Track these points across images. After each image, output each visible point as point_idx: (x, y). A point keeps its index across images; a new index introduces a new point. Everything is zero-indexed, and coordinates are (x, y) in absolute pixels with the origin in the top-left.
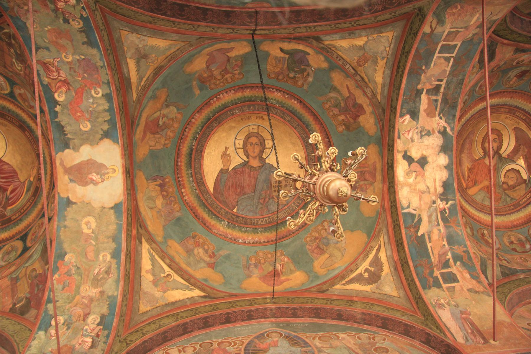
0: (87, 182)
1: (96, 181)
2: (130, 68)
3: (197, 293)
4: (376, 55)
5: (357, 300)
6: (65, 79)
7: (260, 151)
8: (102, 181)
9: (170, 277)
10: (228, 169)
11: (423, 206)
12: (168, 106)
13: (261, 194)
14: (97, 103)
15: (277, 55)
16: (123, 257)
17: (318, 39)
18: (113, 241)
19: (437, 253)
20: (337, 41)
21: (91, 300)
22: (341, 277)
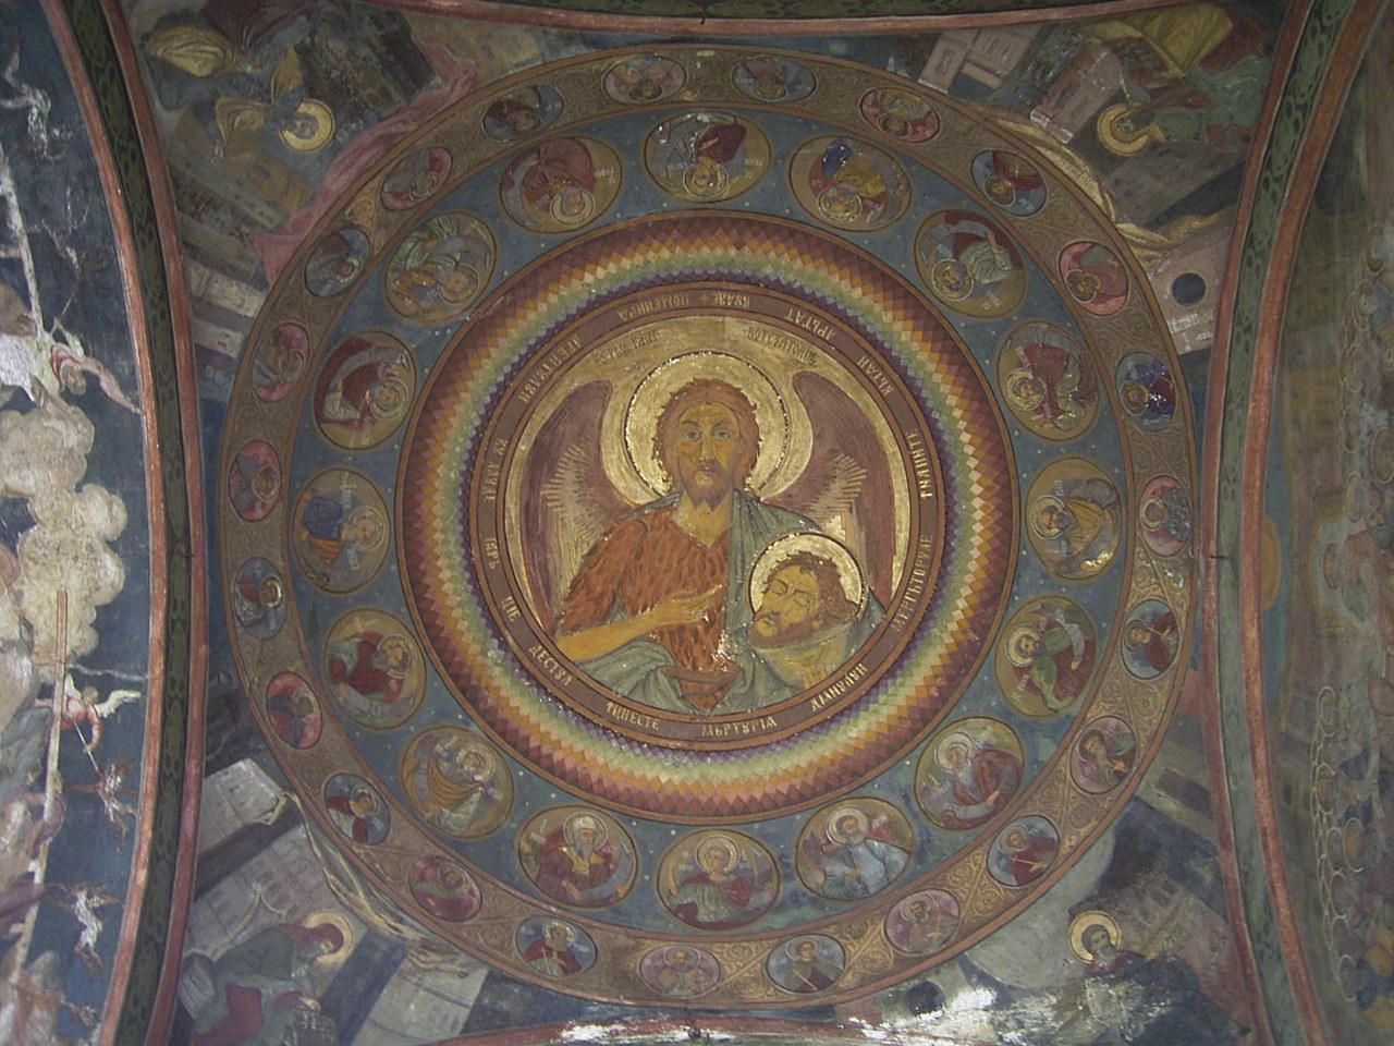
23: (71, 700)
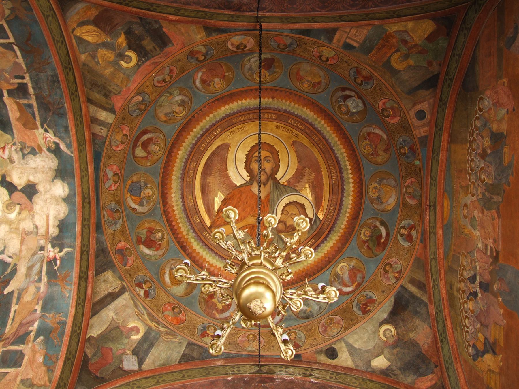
19: (19, 321)
23: (51, 252)
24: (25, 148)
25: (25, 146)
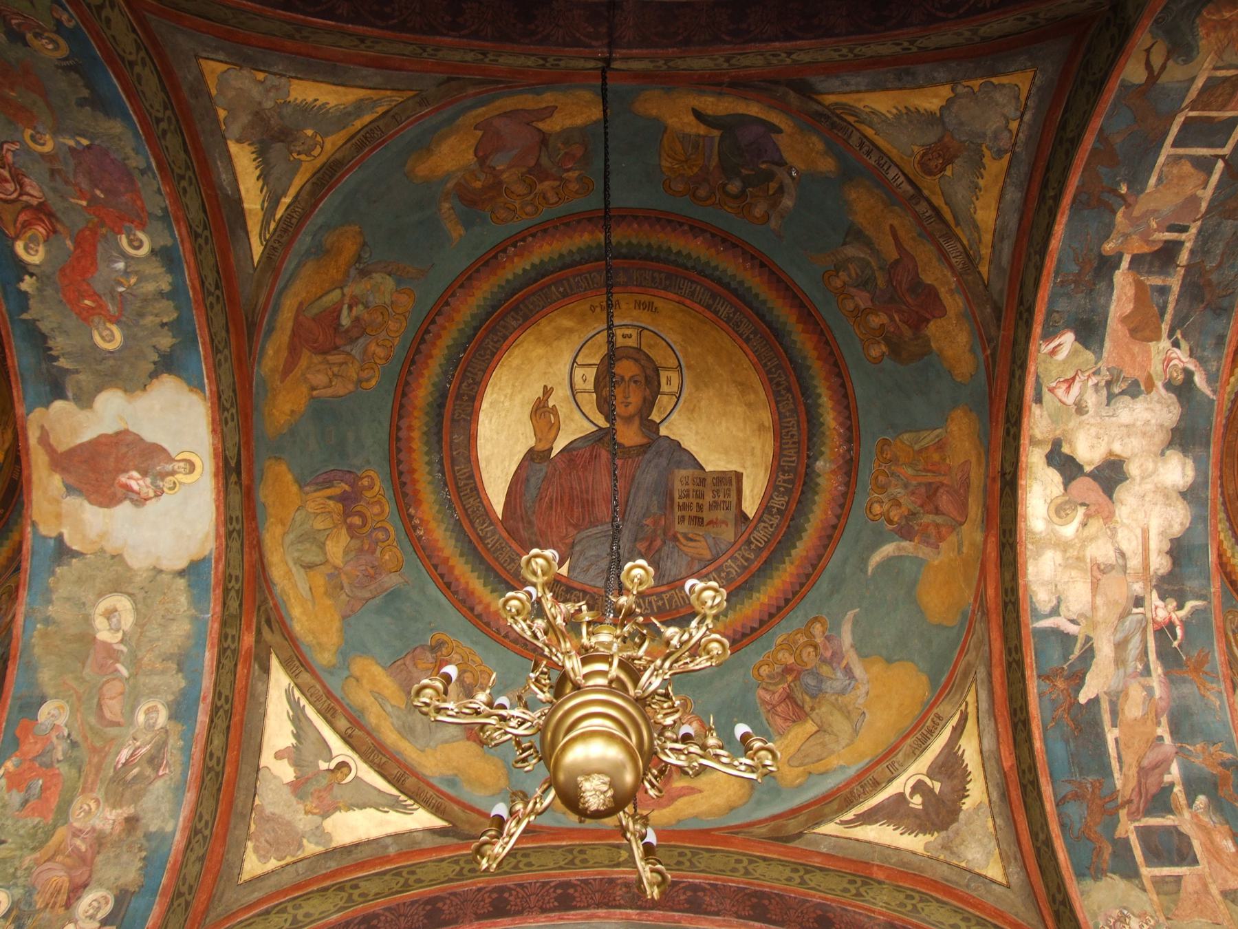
0: (114, 494)
1: (139, 493)
2: (239, 169)
3: (422, 819)
4: (979, 141)
5: (881, 877)
6: (40, 204)
7: (645, 400)
8: (157, 496)
9: (345, 770)
10: (551, 449)
11: (1101, 612)
12: (364, 273)
13: (640, 526)
14: (136, 273)
15: (688, 130)
16: (203, 718)
17: (806, 90)
18: (180, 670)
19: (1135, 763)
20: (860, 95)
21: (100, 841)
22: (841, 799)
24: (1118, 380)
25: (1119, 377)
